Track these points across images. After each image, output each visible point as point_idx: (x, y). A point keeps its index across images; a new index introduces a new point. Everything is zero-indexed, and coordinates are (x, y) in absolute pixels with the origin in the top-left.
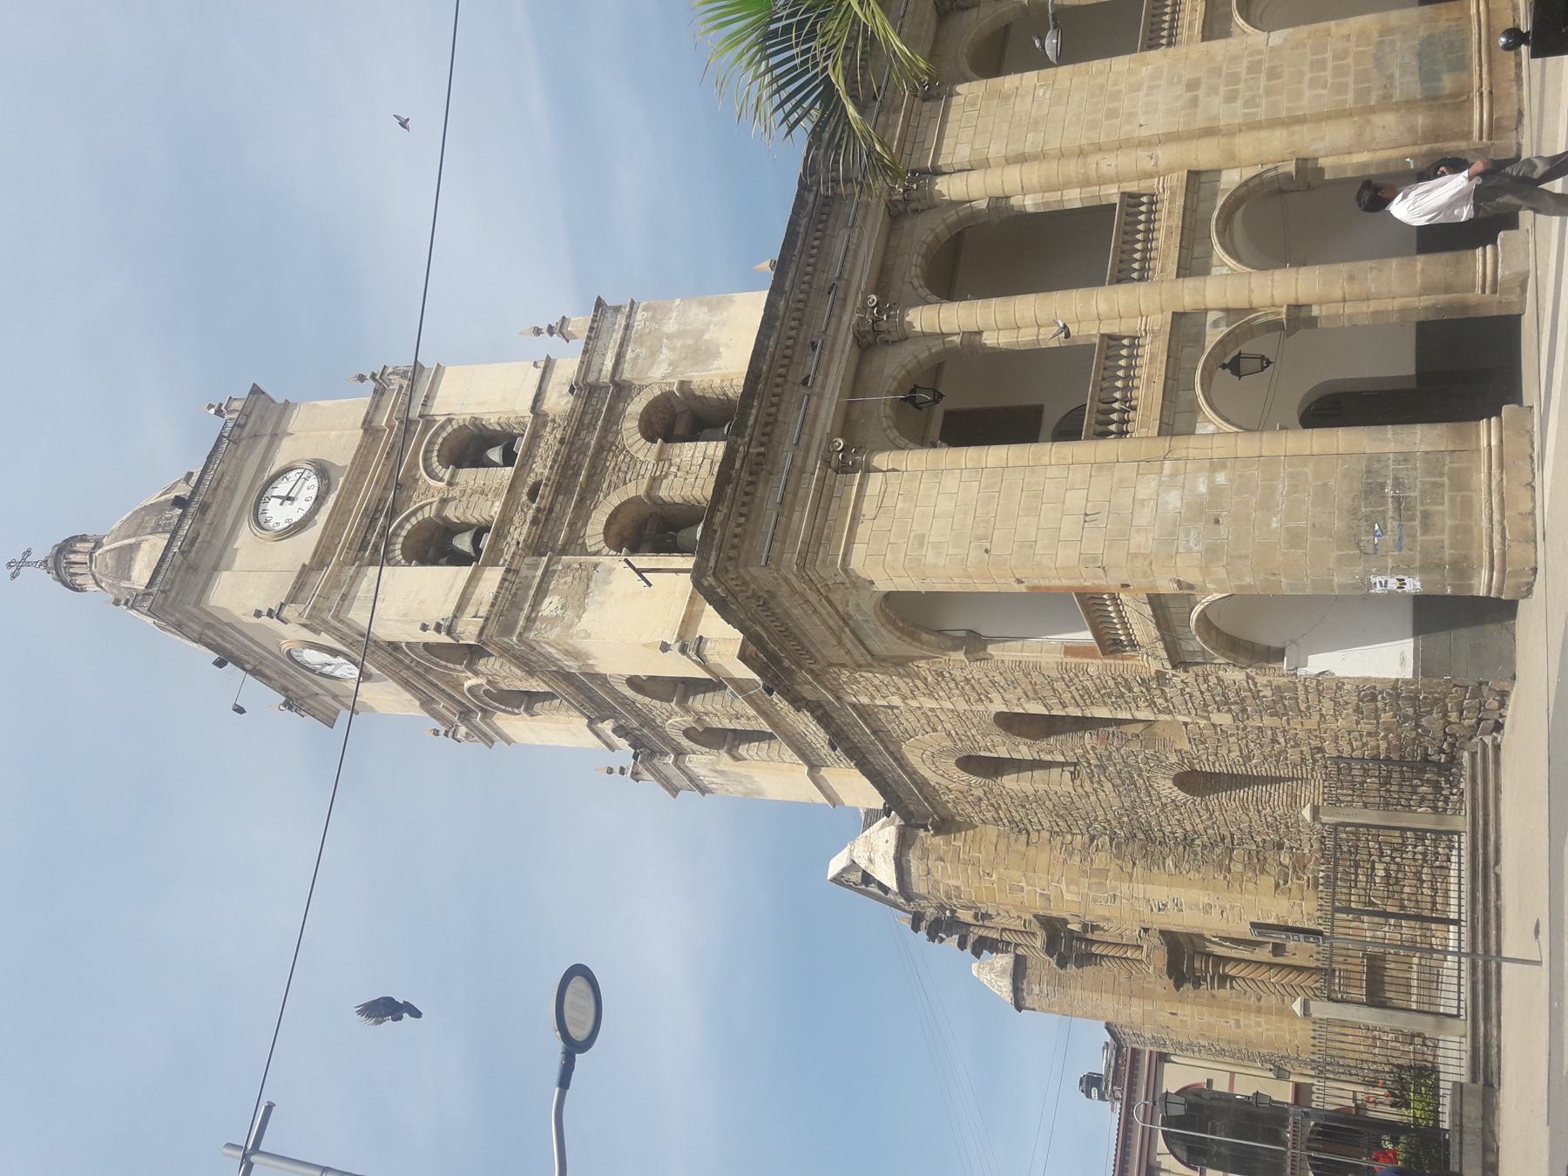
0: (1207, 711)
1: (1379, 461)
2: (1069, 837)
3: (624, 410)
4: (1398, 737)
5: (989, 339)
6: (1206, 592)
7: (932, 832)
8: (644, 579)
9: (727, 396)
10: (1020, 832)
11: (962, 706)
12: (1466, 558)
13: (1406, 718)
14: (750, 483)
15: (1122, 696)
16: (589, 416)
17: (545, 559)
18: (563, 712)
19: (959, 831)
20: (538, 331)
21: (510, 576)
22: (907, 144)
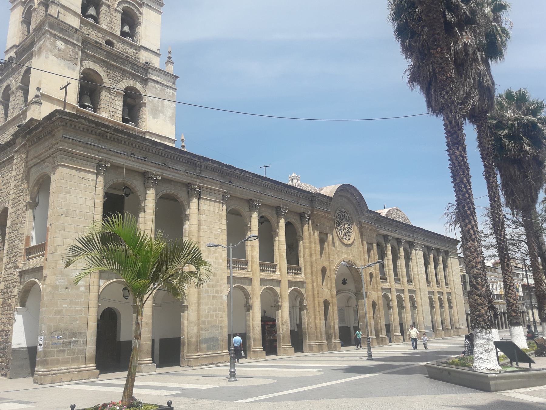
0: (5, 281)
1: (84, 336)
3: (138, 81)
5: (142, 215)
6: (43, 284)
8: (63, 88)
11: (11, 197)
12: (47, 364)
14: (96, 132)
15: (11, 253)
16: (136, 68)
17: (80, 45)
18: (22, 35)
20: (170, 53)
21: (75, 30)
22: (209, 190)
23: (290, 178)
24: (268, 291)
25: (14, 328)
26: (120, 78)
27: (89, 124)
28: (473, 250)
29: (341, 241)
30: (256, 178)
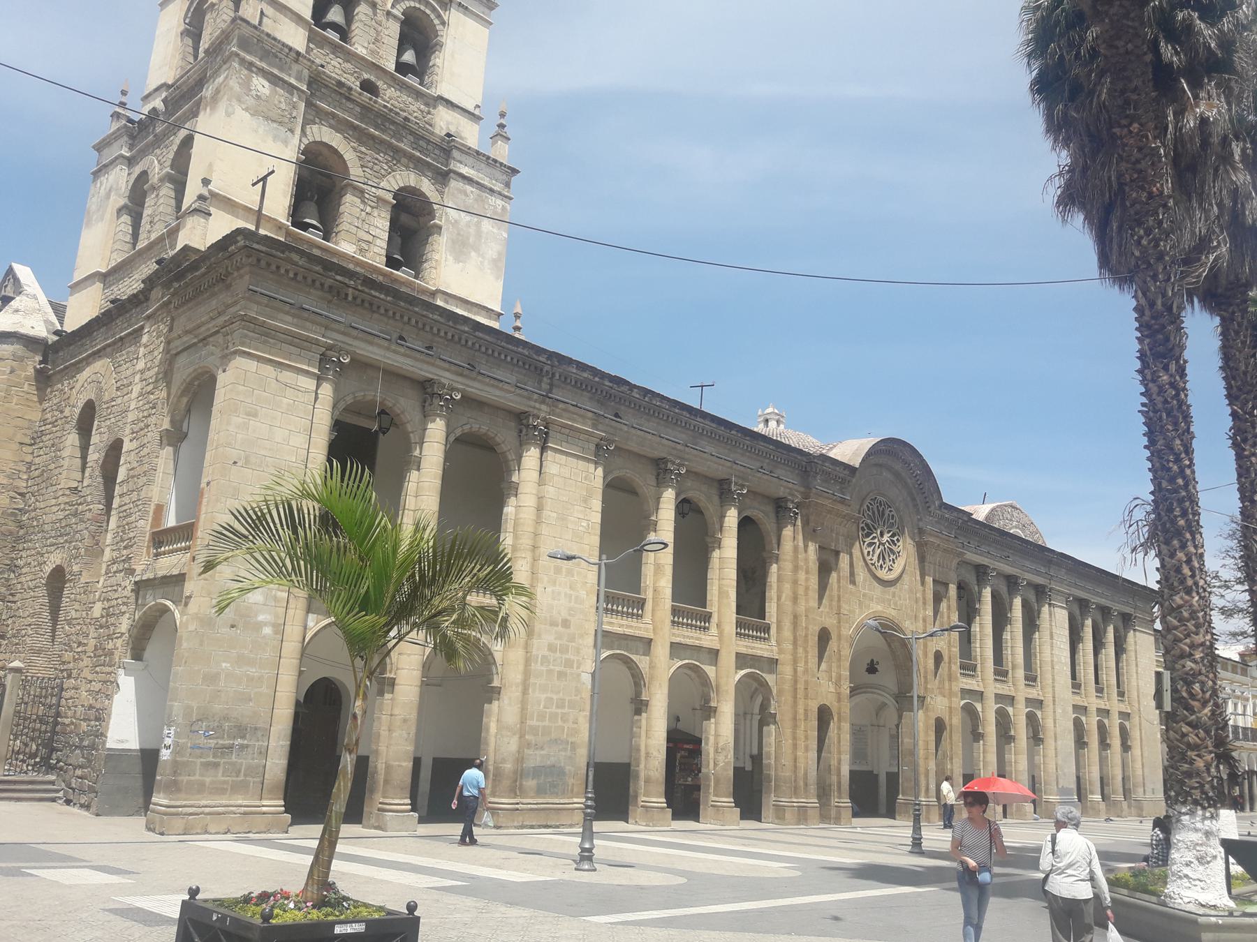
2: (25, 477)
3: (426, 176)
4: (71, 732)
5: (414, 475)
6: (182, 614)
7: (38, 367)
9: (425, 262)
10: (33, 438)
11: (131, 417)
12: (179, 790)
13: (81, 740)
14: (322, 285)
15: (122, 541)
17: (304, 88)
18: (180, 63)
19: (38, 389)
20: (502, 115)
21: (295, 56)
22: (568, 431)
23: (760, 416)
24: (689, 672)
25: (114, 705)
26: (386, 168)
27: (307, 265)
28: (1186, 614)
29: (870, 570)
30: (677, 411)
